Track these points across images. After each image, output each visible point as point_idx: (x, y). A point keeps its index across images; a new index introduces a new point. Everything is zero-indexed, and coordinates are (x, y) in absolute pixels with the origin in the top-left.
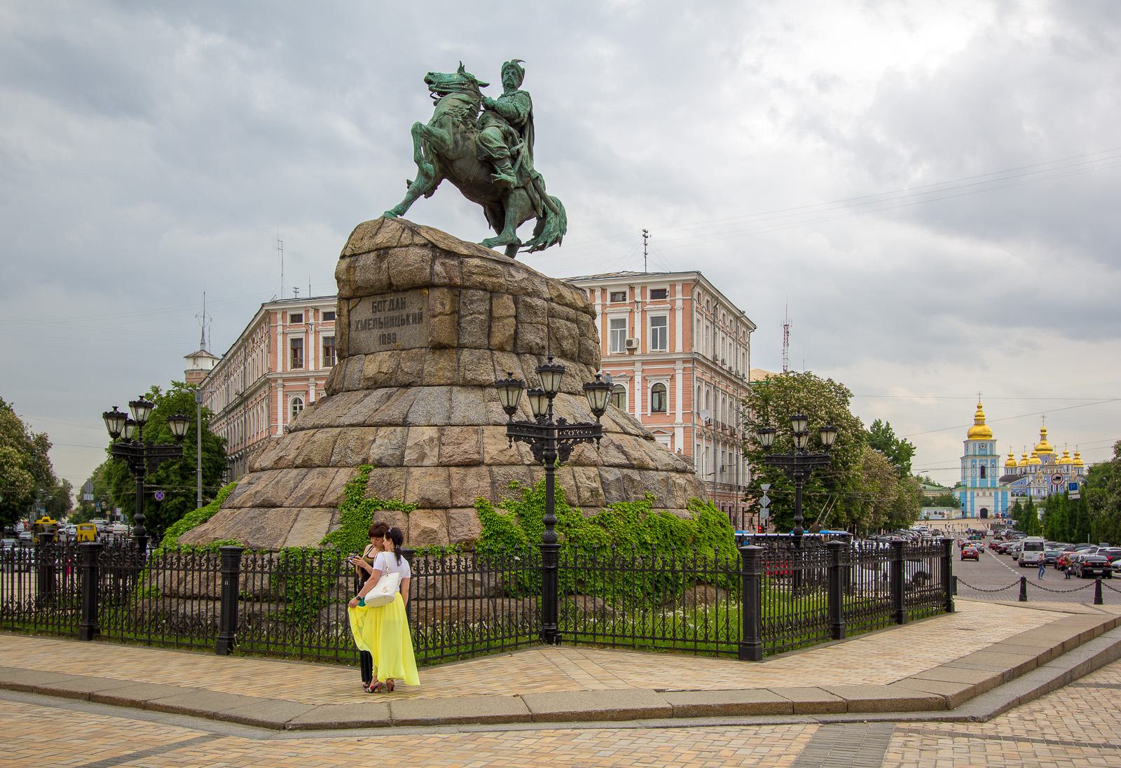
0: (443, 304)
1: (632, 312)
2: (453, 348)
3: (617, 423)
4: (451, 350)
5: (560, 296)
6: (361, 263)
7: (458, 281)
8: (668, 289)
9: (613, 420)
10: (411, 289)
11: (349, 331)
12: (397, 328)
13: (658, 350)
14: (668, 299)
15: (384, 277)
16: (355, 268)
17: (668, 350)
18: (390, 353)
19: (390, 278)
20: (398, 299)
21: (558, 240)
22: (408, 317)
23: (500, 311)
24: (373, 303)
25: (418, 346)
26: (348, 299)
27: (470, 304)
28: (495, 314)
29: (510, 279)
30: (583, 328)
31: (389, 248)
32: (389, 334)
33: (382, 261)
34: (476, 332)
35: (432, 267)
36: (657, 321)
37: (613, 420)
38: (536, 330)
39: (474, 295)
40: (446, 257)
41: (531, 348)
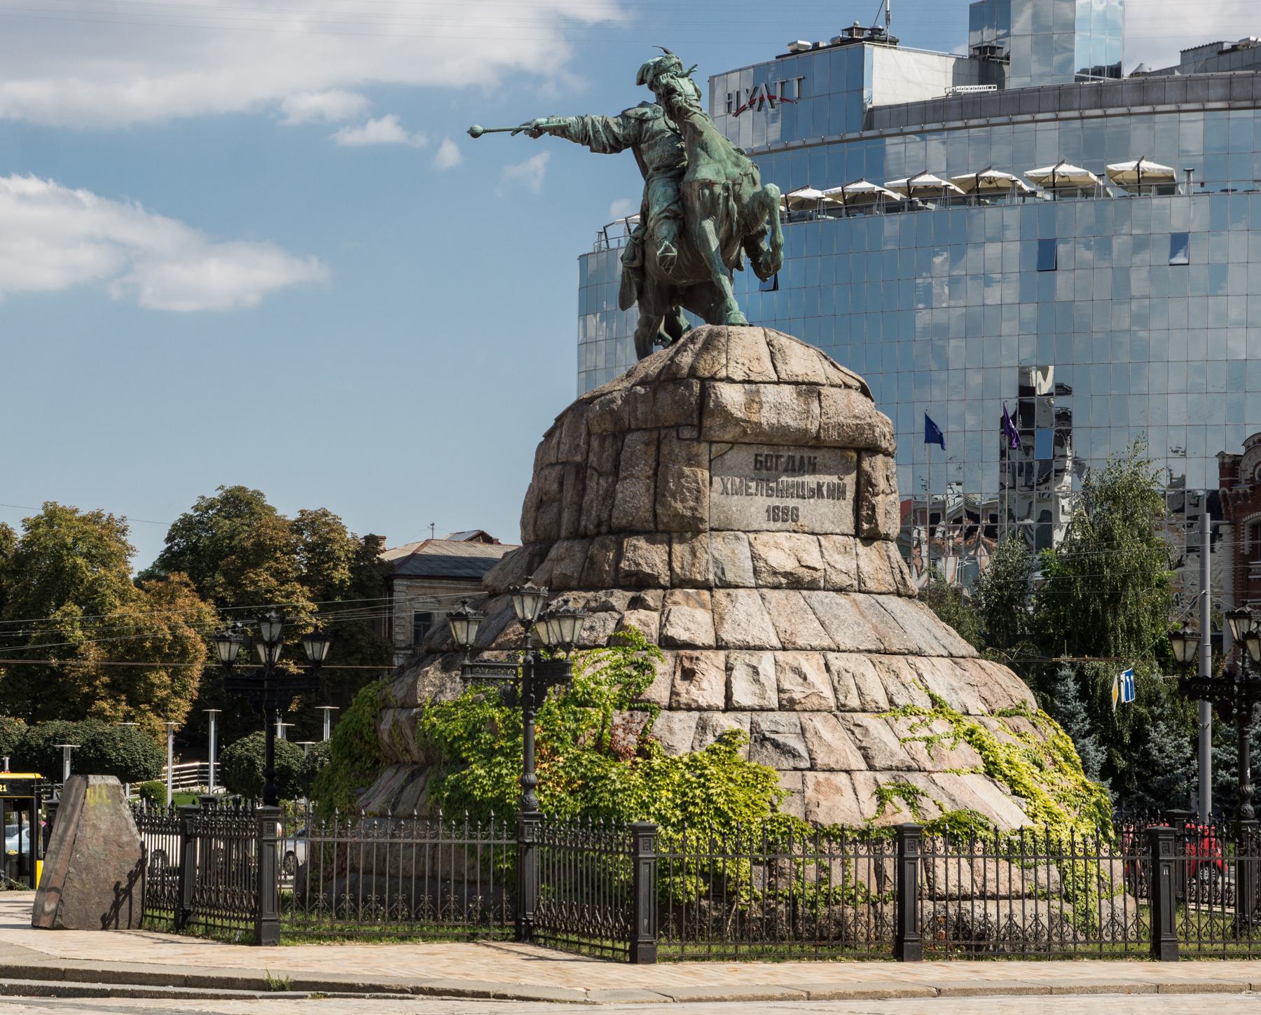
6: (771, 398)
20: (802, 457)
22: (820, 486)
24: (757, 455)
25: (838, 531)
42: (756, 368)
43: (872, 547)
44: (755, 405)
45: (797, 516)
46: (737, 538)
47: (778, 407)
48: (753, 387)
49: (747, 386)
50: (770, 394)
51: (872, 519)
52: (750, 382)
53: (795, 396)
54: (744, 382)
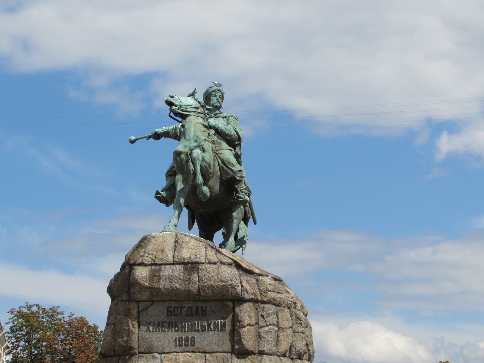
0: (250, 317)
2: (254, 354)
4: (253, 356)
6: (166, 273)
10: (214, 300)
11: (139, 330)
12: (197, 333)
15: (194, 288)
16: (159, 277)
18: (193, 355)
19: (199, 291)
20: (197, 307)
23: (284, 323)
24: (168, 308)
25: (221, 350)
26: (138, 302)
27: (267, 317)
28: (281, 326)
29: (287, 295)
31: (198, 263)
32: (187, 338)
33: (190, 274)
34: (272, 341)
35: (242, 286)
38: (301, 338)
39: (270, 309)
40: (246, 275)
41: (301, 353)
42: (160, 256)
43: (247, 359)
44: (156, 278)
45: (194, 342)
46: (154, 357)
47: (171, 278)
48: (157, 267)
49: (153, 267)
50: (167, 271)
51: (240, 342)
52: (156, 265)
53: (182, 271)
54: (151, 265)
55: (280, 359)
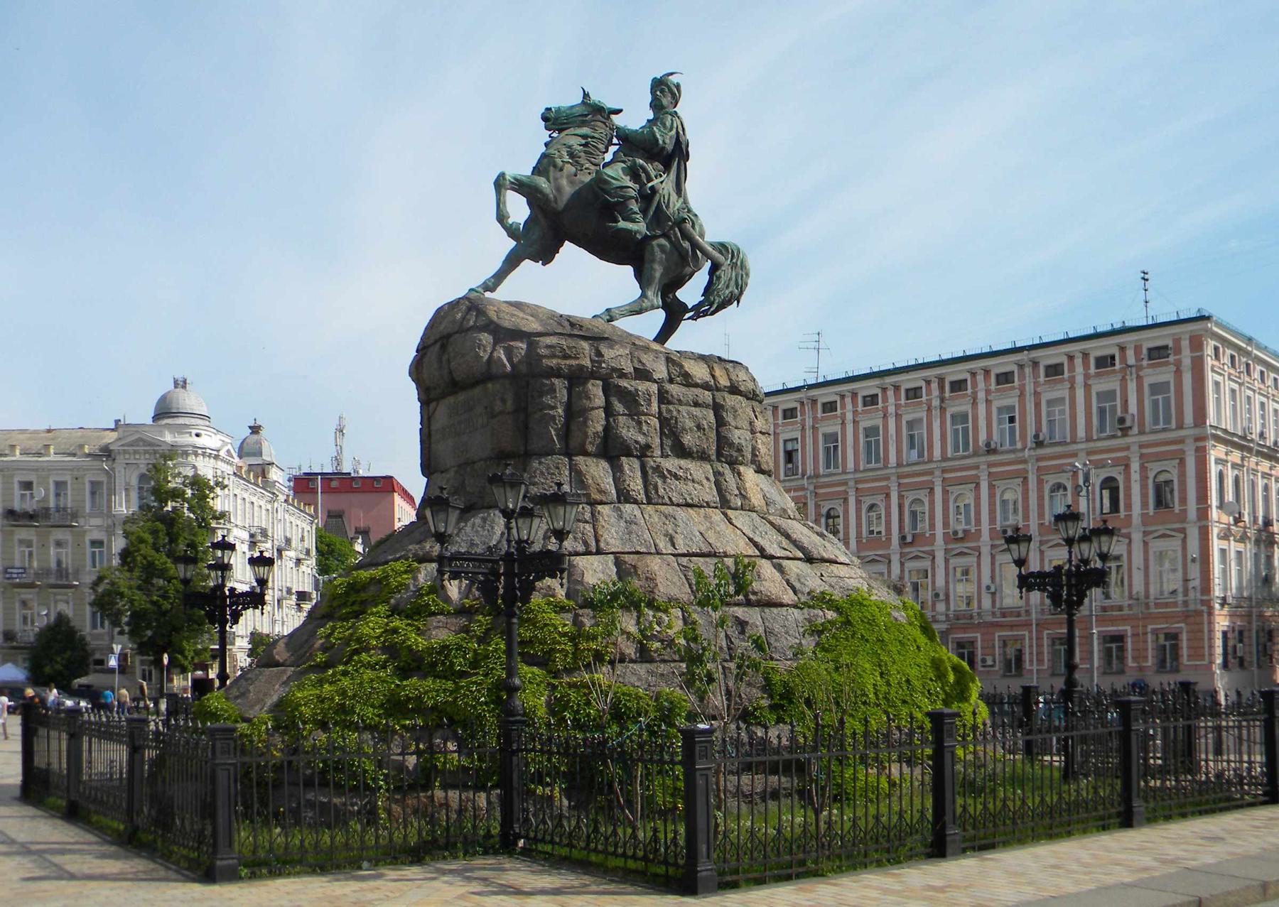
0: (503, 401)
1: (1124, 379)
3: (756, 545)
5: (686, 375)
7: (524, 369)
8: (1171, 345)
9: (751, 540)
13: (1161, 426)
14: (1171, 359)
17: (1173, 425)
19: (451, 372)
21: (735, 298)
30: (724, 414)
31: (449, 336)
36: (1157, 388)
37: (751, 540)
55: (571, 460)
